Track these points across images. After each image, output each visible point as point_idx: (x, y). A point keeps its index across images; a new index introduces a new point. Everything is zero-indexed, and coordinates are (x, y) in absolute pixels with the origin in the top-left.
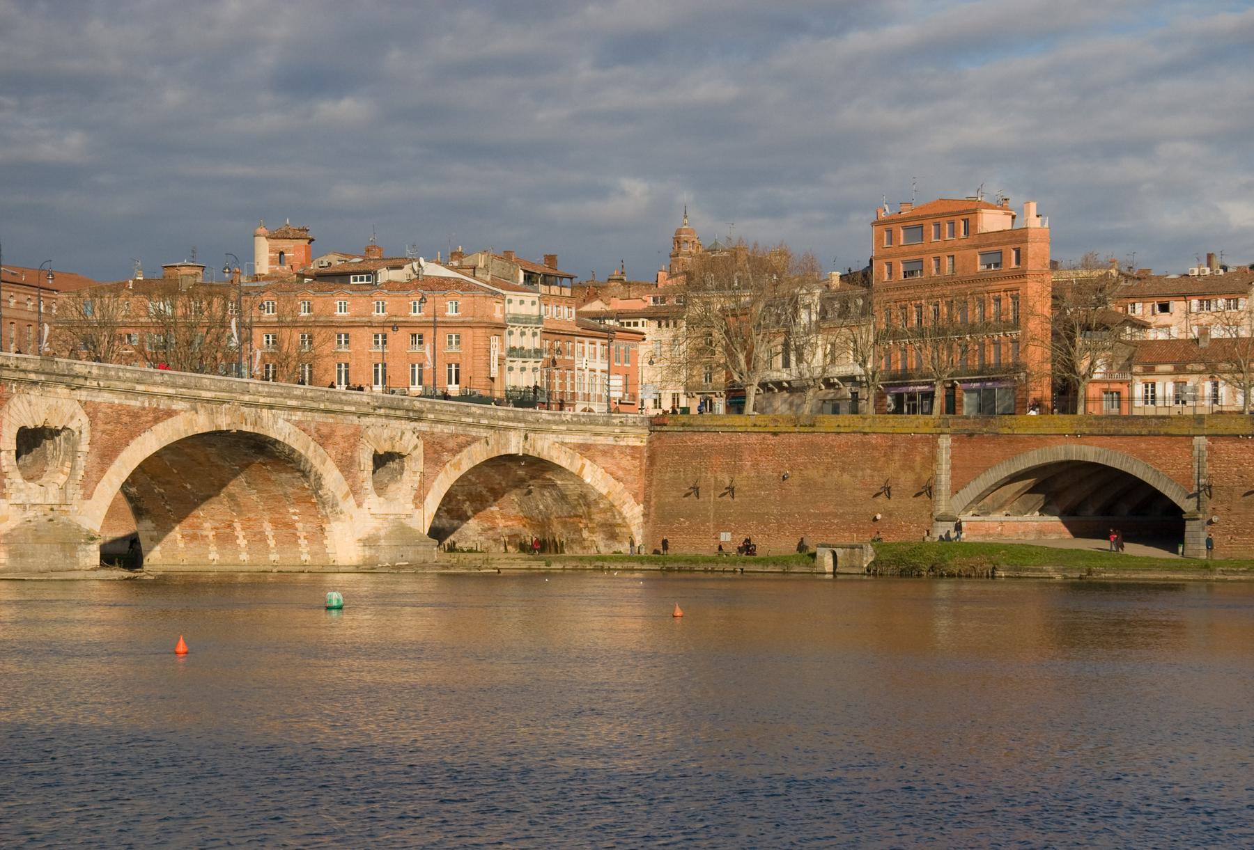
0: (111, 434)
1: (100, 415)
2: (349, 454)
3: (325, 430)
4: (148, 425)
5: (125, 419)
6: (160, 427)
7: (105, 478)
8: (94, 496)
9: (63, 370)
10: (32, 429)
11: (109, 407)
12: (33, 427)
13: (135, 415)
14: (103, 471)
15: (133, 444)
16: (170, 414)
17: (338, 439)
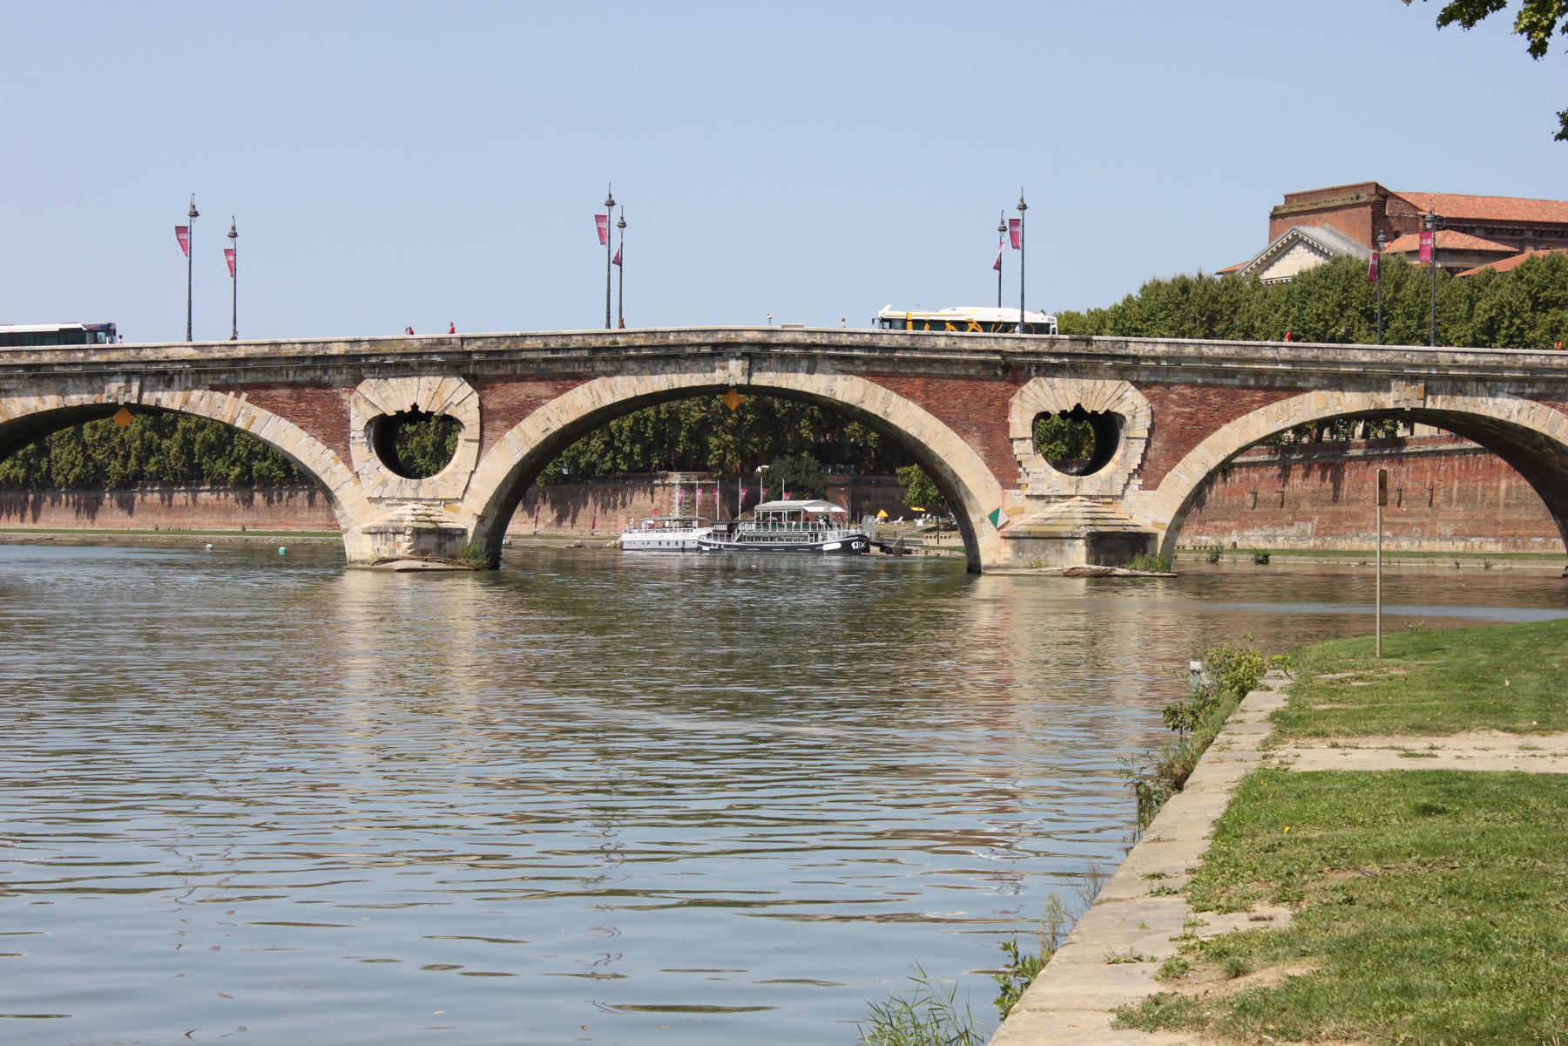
0: (1191, 417)
4: (1255, 406)
14: (1177, 458)
15: (1226, 428)
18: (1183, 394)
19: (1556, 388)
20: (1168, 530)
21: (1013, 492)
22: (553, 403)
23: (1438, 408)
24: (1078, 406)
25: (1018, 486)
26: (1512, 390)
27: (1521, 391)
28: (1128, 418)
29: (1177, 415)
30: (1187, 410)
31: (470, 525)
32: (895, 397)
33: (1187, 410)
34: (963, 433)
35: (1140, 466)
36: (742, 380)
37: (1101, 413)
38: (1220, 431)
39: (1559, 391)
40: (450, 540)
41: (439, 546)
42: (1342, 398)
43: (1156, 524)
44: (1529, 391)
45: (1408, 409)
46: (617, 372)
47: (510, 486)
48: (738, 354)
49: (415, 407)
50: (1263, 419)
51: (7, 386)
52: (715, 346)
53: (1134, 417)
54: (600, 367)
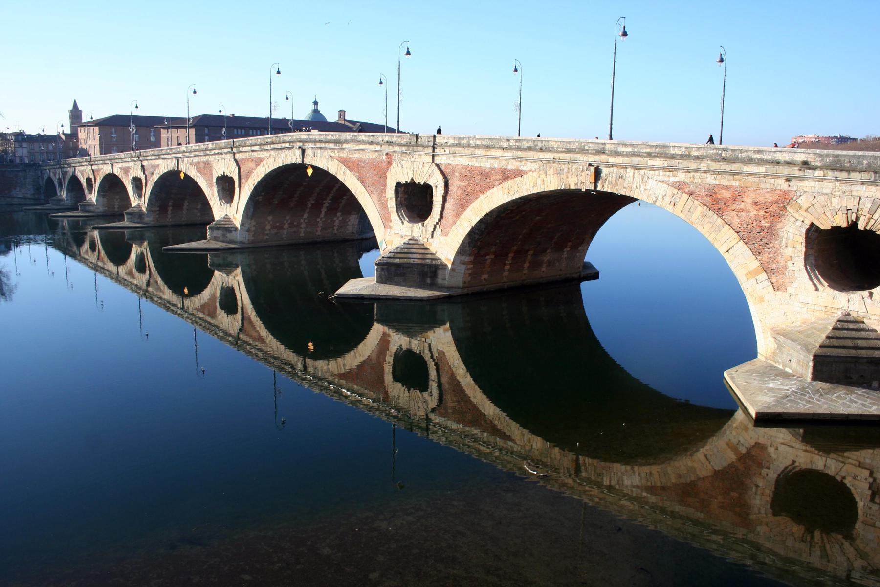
1: (457, 174)
2: (765, 223)
3: (724, 194)
4: (497, 182)
5: (478, 177)
6: (508, 184)
7: (458, 222)
8: (450, 235)
9: (425, 142)
10: (404, 184)
11: (463, 168)
12: (404, 183)
13: (485, 174)
14: (457, 216)
15: (482, 197)
16: (519, 173)
17: (747, 203)
18: (461, 173)
19: (694, 178)
20: (453, 264)
21: (389, 230)
22: (255, 172)
23: (605, 190)
24: (412, 179)
25: (390, 227)
26: (661, 178)
27: (666, 179)
28: (434, 188)
29: (459, 187)
30: (463, 184)
31: (238, 226)
32: (348, 172)
33: (463, 184)
34: (370, 193)
35: (440, 220)
36: (299, 161)
37: (422, 184)
38: (479, 199)
39: (696, 181)
40: (229, 233)
41: (224, 235)
42: (545, 179)
43: (448, 259)
44: (672, 179)
45: (583, 190)
46: (270, 157)
47: (252, 210)
48: (298, 147)
49: (224, 173)
50: (501, 192)
51: (160, 163)
52: (289, 142)
53: (436, 187)
54: (266, 154)
